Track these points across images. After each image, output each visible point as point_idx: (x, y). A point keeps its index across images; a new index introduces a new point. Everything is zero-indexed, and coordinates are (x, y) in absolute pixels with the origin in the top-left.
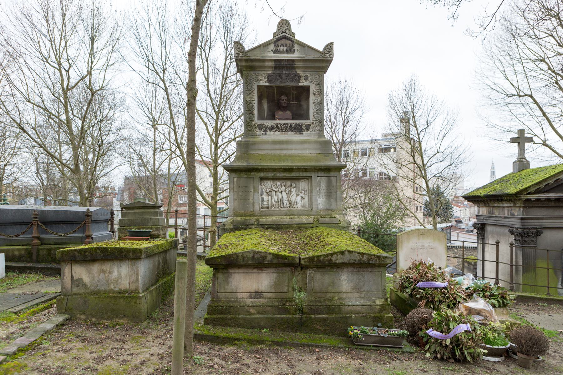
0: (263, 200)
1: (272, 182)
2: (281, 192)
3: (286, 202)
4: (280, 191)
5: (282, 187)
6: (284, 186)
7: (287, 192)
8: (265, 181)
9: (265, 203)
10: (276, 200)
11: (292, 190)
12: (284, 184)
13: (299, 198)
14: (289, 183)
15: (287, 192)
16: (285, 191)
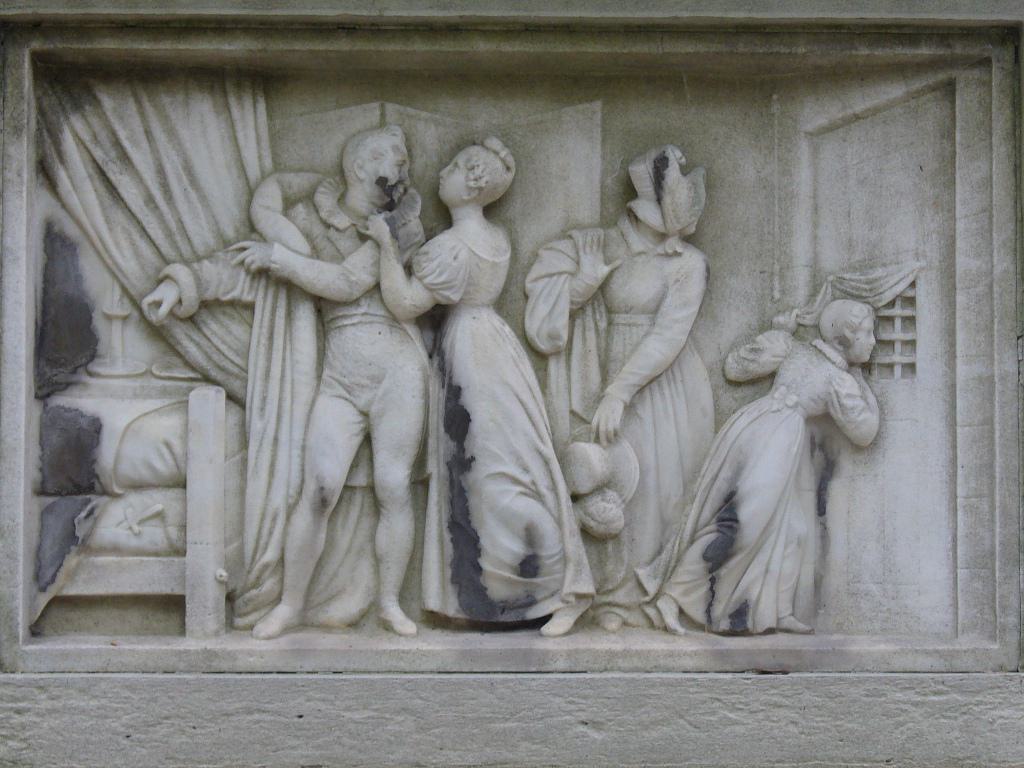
0: (72, 470)
1: (250, 117)
2: (435, 320)
3: (511, 502)
4: (412, 296)
5: (442, 217)
6: (492, 210)
7: (547, 315)
8: (120, 112)
9: (116, 520)
10: (334, 468)
11: (638, 286)
12: (487, 166)
13: (770, 447)
14: (575, 154)
15: (547, 315)
16: (510, 303)
